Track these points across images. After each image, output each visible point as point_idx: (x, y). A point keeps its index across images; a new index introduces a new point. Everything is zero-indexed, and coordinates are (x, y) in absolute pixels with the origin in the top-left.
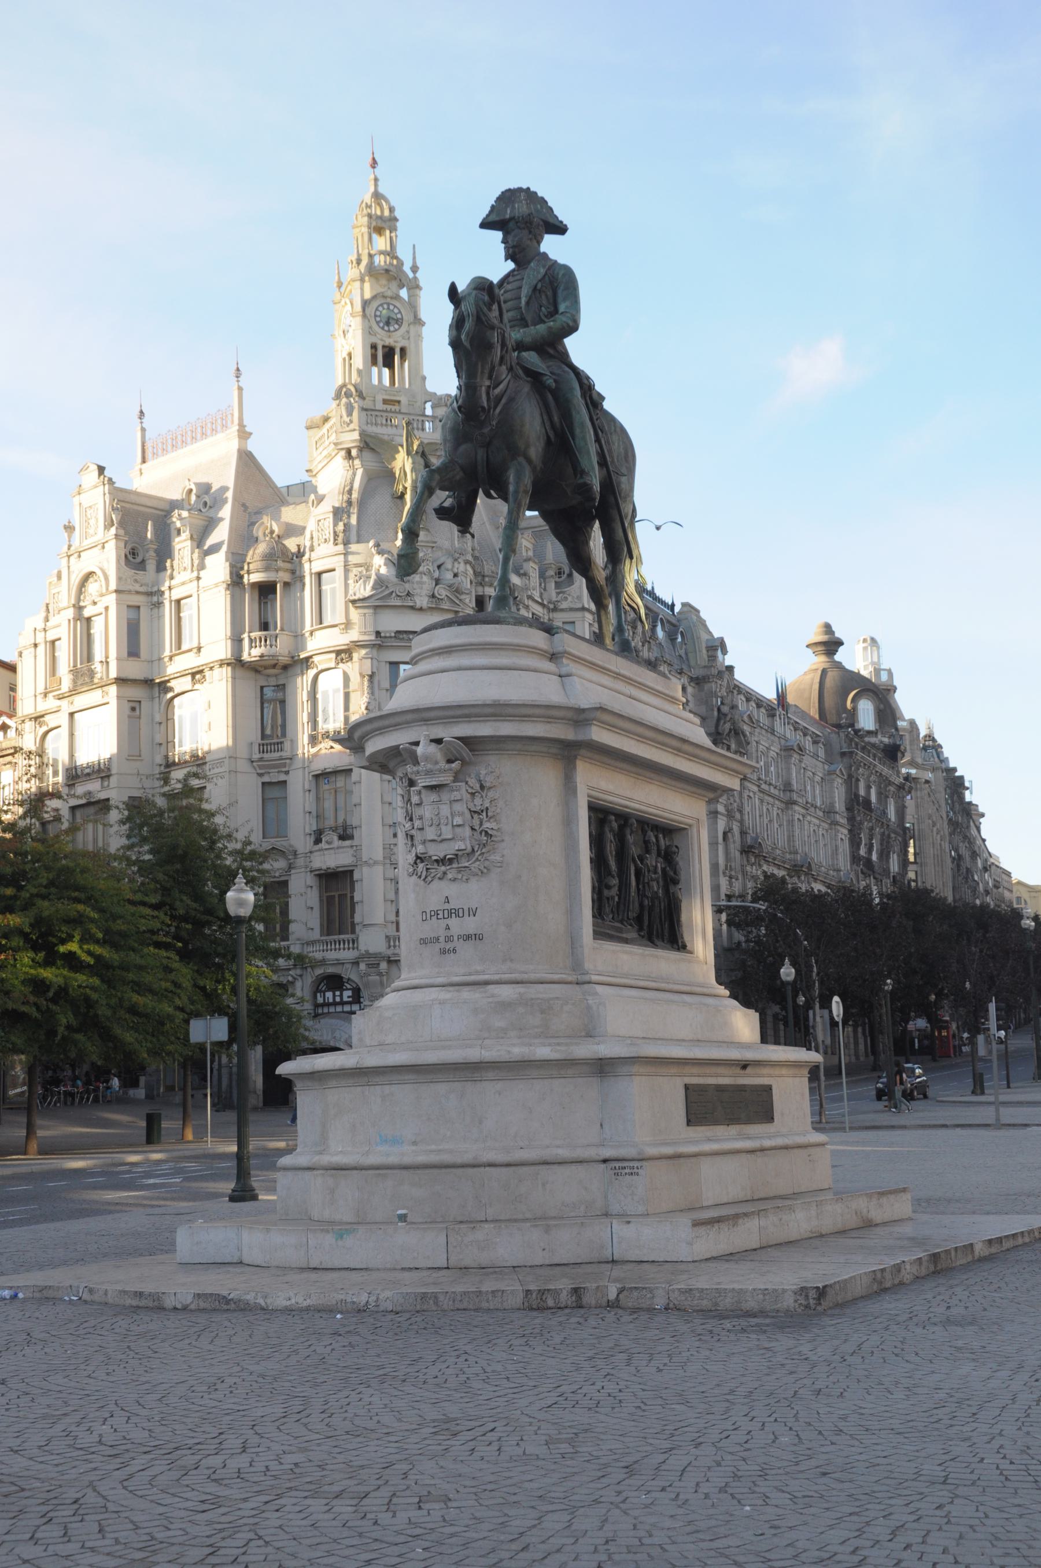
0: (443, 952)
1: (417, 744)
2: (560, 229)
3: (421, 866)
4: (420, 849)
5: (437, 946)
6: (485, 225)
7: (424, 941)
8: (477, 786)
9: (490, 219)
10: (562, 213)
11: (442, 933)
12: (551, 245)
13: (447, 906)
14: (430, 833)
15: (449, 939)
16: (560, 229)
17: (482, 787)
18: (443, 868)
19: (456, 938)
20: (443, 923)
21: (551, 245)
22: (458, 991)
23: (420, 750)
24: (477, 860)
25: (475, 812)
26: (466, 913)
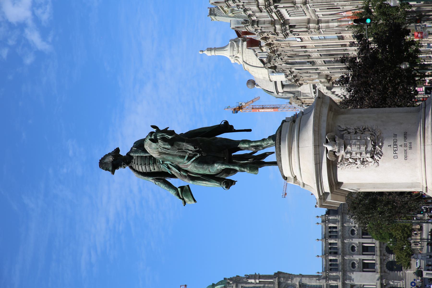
0: (411, 148)
1: (327, 150)
2: (118, 150)
3: (375, 157)
4: (368, 155)
5: (408, 151)
6: (113, 173)
7: (406, 158)
8: (345, 131)
9: (111, 169)
10: (111, 150)
11: (402, 149)
12: (123, 153)
13: (392, 146)
14: (363, 148)
15: (405, 146)
16: (118, 150)
17: (345, 130)
18: (377, 147)
19: (405, 142)
20: (399, 148)
21: (123, 153)
22: (427, 138)
23: (330, 148)
24: (375, 133)
25: (356, 132)
26: (395, 138)
